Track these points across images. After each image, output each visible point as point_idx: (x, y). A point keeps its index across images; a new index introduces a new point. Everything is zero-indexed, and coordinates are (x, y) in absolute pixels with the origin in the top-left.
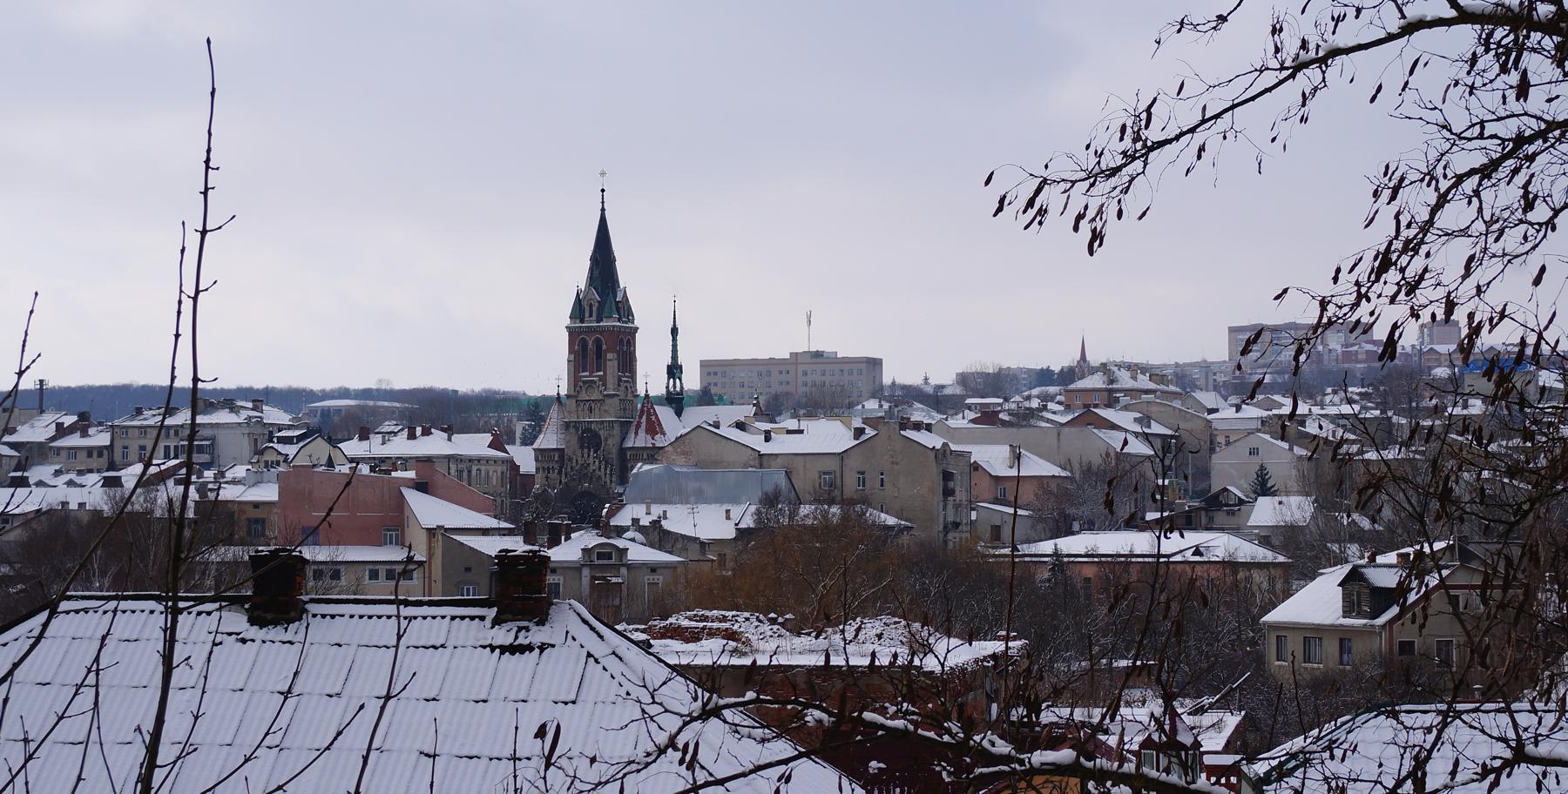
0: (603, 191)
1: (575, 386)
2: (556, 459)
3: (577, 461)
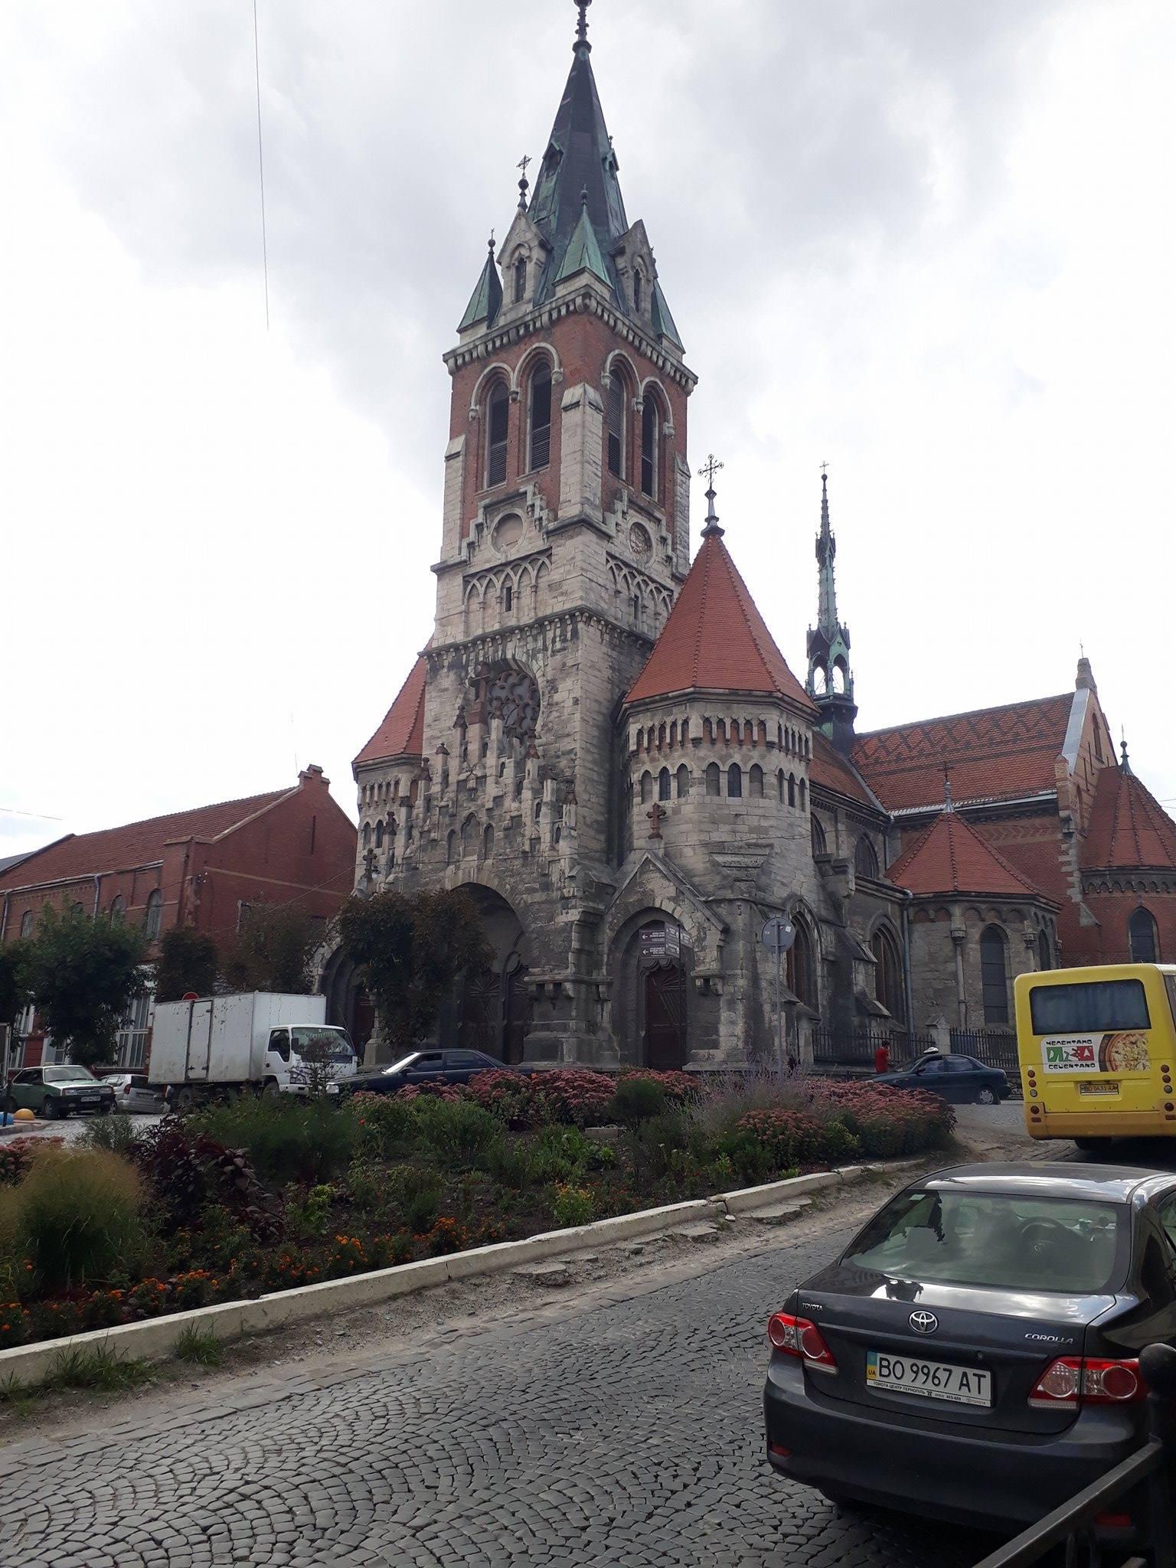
1: (464, 534)
2: (403, 791)
3: (446, 775)
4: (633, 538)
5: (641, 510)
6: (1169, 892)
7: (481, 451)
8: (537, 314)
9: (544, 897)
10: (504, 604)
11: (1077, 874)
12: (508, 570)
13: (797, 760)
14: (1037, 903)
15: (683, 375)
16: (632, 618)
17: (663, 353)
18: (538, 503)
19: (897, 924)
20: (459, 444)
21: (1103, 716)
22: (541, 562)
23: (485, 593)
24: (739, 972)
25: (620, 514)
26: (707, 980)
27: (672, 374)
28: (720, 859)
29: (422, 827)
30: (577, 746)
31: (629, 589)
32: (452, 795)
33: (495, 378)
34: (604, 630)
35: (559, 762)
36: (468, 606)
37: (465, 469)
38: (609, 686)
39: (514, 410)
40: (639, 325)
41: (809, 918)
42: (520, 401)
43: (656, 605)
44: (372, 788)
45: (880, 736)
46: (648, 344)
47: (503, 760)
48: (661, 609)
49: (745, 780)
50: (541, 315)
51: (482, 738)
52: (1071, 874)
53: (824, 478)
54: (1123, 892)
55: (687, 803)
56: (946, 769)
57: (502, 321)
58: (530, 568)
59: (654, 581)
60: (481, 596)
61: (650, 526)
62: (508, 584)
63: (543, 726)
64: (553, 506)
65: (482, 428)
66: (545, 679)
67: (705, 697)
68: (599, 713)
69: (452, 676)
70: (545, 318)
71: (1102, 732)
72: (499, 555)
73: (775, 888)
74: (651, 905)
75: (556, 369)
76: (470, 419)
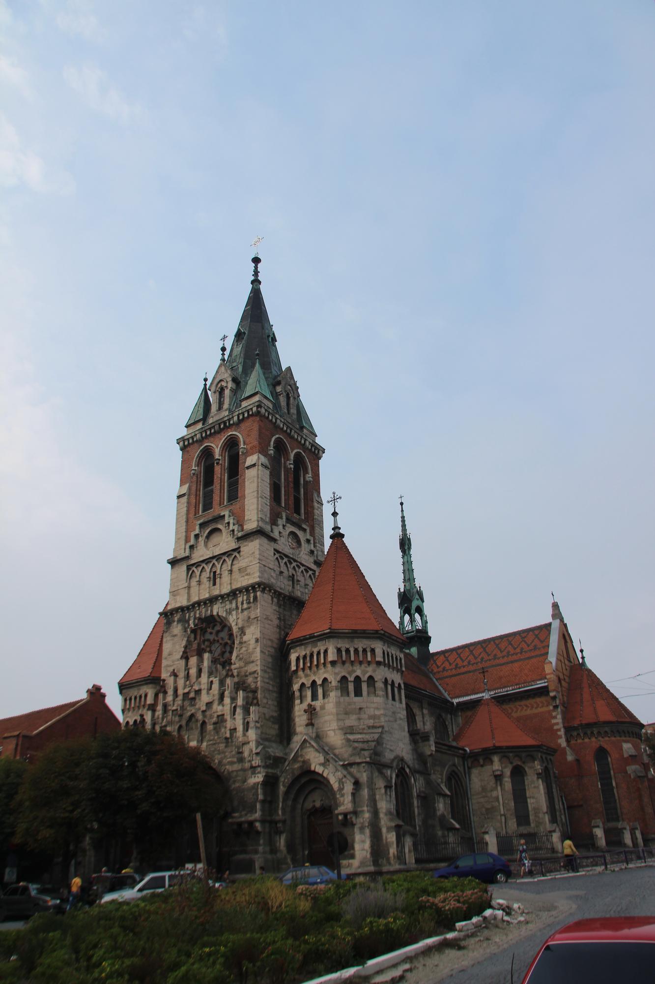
0: (256, 261)
1: (187, 540)
2: (150, 700)
3: (176, 690)
4: (290, 540)
5: (294, 524)
6: (615, 737)
7: (198, 493)
8: (231, 417)
9: (240, 767)
10: (212, 582)
11: (562, 730)
12: (214, 561)
13: (395, 672)
14: (541, 750)
15: (316, 448)
16: (291, 588)
17: (304, 436)
18: (232, 521)
19: (461, 769)
20: (185, 489)
21: (569, 635)
22: (233, 556)
23: (200, 575)
24: (365, 808)
25: (281, 527)
26: (345, 815)
27: (310, 447)
28: (351, 737)
29: (161, 723)
30: (258, 668)
31: (288, 571)
32: (180, 702)
33: (207, 451)
34: (273, 596)
35: (247, 679)
36: (190, 583)
37: (188, 503)
38: (278, 630)
39: (217, 469)
40: (290, 422)
41: (407, 770)
42: (221, 464)
43: (305, 580)
44: (130, 699)
45: (443, 653)
46: (295, 432)
47: (211, 679)
48: (309, 582)
49: (364, 686)
50: (233, 417)
51: (198, 666)
52: (559, 730)
53: (402, 504)
54: (589, 738)
55: (328, 702)
56: (483, 672)
57: (211, 421)
58: (227, 559)
59: (303, 565)
60: (198, 577)
61: (300, 534)
62: (214, 570)
63: (237, 657)
64: (240, 524)
65: (199, 480)
66: (237, 627)
67: (337, 635)
68: (272, 647)
69: (180, 627)
70: (236, 418)
71: (569, 644)
72: (208, 552)
73: (386, 754)
74: (309, 769)
75: (242, 446)
76: (192, 475)
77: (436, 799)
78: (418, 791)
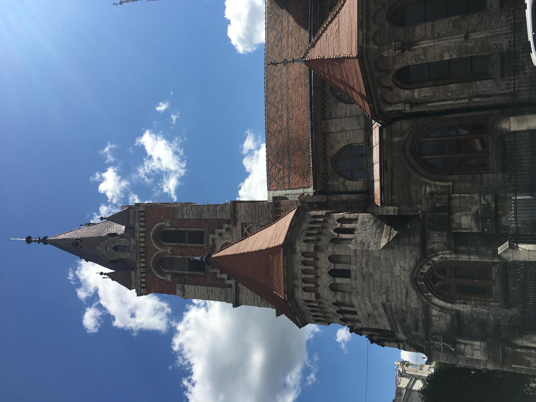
41: (426, 268)
73: (413, 305)
77: (455, 231)
78: (448, 252)
